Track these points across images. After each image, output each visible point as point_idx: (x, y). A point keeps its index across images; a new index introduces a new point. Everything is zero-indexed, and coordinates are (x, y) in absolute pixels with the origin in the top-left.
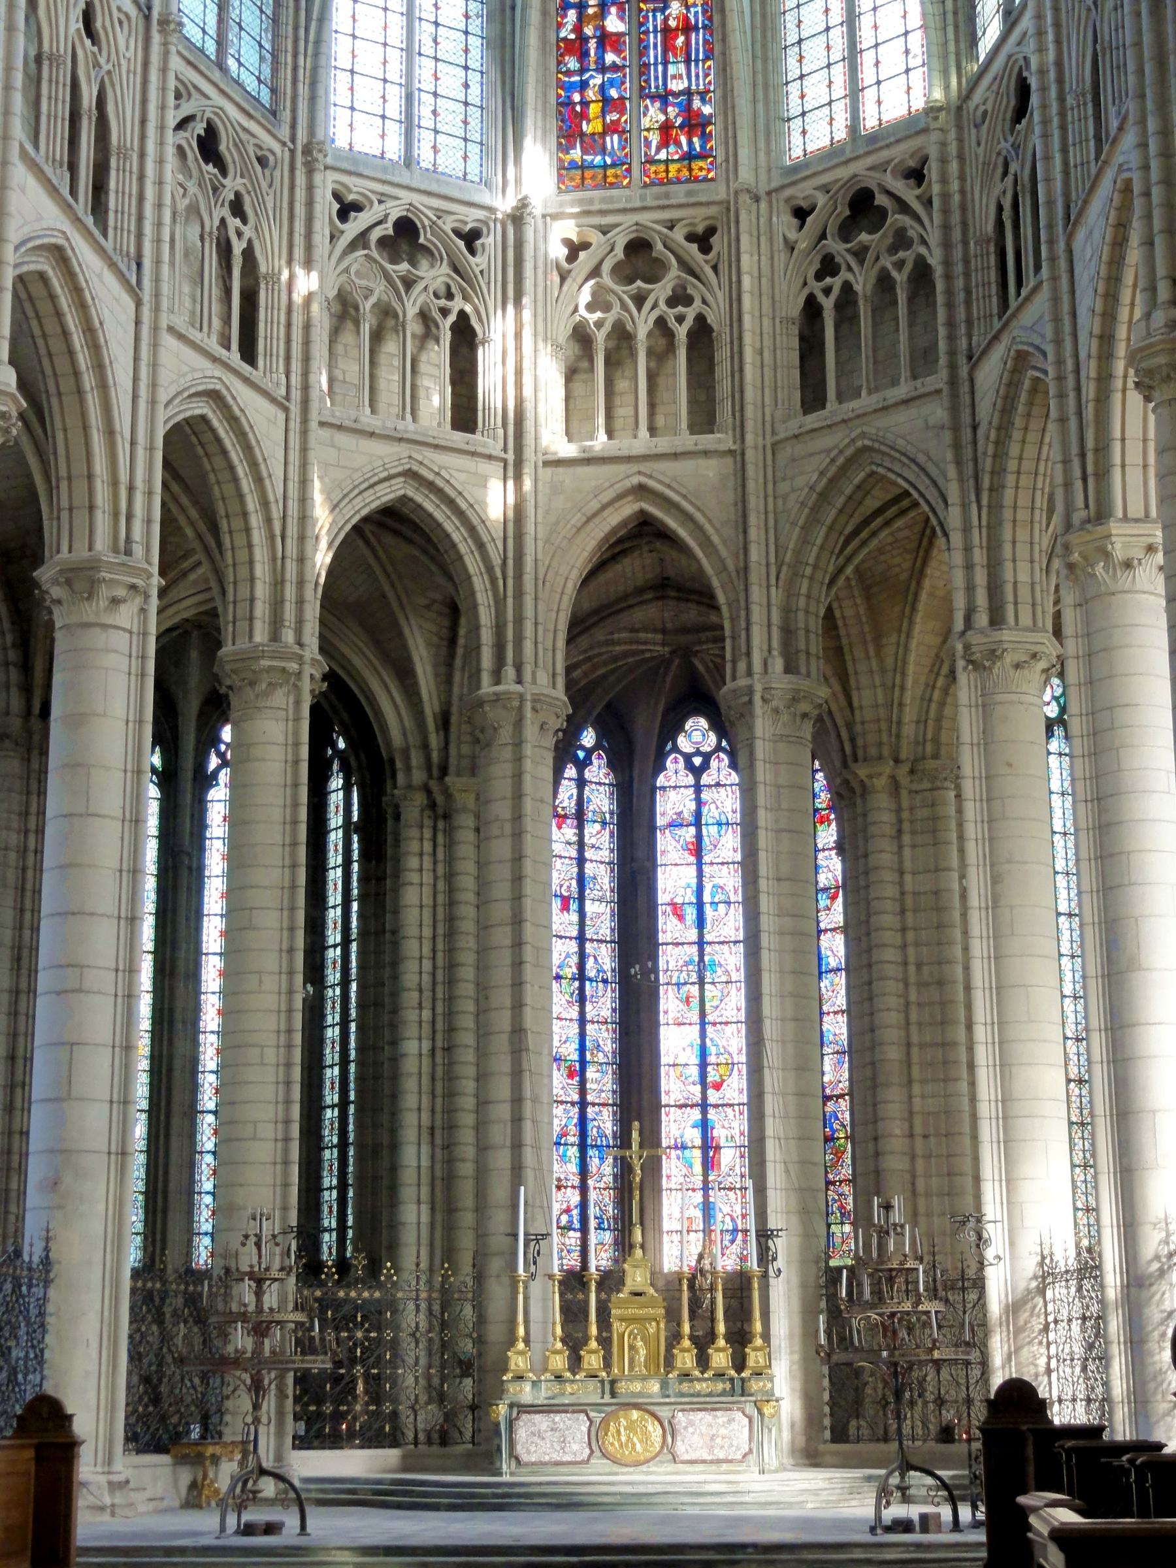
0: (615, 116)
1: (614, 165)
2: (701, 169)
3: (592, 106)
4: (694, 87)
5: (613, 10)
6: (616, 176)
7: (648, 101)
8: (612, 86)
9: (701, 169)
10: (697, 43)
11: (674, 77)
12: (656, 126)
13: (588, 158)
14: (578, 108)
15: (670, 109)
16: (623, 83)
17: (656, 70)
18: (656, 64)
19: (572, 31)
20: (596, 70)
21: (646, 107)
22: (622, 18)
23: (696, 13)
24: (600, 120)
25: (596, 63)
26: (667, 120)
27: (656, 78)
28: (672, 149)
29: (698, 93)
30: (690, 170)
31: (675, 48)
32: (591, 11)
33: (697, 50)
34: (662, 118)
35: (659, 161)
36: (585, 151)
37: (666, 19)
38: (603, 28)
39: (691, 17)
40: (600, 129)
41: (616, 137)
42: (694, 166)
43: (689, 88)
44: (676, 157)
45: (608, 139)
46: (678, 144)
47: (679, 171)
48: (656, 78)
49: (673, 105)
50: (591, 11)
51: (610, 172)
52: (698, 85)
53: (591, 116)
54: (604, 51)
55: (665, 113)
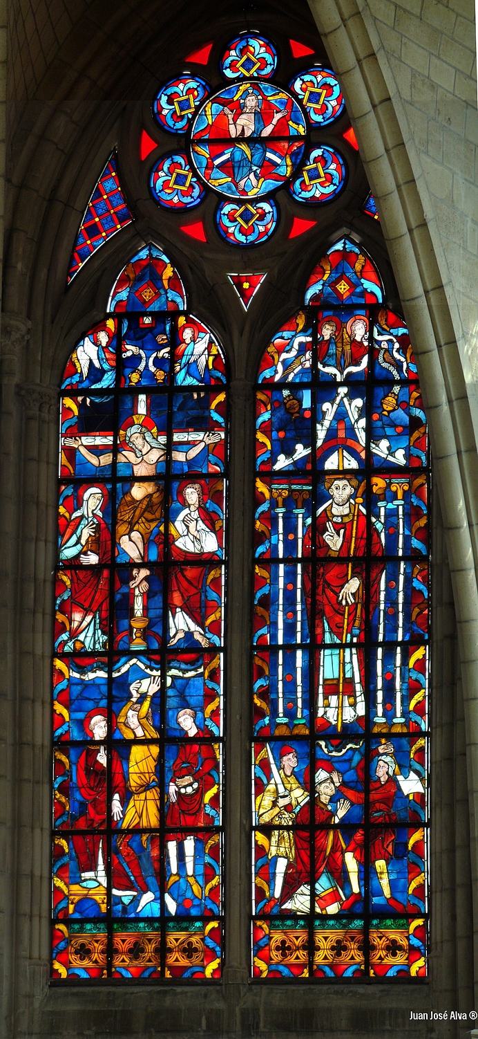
2: (393, 948)
6: (189, 951)
12: (287, 819)
13: (126, 896)
14: (102, 758)
23: (392, 514)
25: (146, 634)
26: (314, 801)
27: (290, 685)
32: (138, 492)
33: (391, 617)
37: (317, 529)
38: (167, 541)
43: (367, 719)
45: (172, 846)
46: (341, 876)
47: (339, 948)
48: (290, 685)
50: (138, 492)
51: (175, 938)
52: (390, 714)
53: (134, 781)
55: (310, 786)
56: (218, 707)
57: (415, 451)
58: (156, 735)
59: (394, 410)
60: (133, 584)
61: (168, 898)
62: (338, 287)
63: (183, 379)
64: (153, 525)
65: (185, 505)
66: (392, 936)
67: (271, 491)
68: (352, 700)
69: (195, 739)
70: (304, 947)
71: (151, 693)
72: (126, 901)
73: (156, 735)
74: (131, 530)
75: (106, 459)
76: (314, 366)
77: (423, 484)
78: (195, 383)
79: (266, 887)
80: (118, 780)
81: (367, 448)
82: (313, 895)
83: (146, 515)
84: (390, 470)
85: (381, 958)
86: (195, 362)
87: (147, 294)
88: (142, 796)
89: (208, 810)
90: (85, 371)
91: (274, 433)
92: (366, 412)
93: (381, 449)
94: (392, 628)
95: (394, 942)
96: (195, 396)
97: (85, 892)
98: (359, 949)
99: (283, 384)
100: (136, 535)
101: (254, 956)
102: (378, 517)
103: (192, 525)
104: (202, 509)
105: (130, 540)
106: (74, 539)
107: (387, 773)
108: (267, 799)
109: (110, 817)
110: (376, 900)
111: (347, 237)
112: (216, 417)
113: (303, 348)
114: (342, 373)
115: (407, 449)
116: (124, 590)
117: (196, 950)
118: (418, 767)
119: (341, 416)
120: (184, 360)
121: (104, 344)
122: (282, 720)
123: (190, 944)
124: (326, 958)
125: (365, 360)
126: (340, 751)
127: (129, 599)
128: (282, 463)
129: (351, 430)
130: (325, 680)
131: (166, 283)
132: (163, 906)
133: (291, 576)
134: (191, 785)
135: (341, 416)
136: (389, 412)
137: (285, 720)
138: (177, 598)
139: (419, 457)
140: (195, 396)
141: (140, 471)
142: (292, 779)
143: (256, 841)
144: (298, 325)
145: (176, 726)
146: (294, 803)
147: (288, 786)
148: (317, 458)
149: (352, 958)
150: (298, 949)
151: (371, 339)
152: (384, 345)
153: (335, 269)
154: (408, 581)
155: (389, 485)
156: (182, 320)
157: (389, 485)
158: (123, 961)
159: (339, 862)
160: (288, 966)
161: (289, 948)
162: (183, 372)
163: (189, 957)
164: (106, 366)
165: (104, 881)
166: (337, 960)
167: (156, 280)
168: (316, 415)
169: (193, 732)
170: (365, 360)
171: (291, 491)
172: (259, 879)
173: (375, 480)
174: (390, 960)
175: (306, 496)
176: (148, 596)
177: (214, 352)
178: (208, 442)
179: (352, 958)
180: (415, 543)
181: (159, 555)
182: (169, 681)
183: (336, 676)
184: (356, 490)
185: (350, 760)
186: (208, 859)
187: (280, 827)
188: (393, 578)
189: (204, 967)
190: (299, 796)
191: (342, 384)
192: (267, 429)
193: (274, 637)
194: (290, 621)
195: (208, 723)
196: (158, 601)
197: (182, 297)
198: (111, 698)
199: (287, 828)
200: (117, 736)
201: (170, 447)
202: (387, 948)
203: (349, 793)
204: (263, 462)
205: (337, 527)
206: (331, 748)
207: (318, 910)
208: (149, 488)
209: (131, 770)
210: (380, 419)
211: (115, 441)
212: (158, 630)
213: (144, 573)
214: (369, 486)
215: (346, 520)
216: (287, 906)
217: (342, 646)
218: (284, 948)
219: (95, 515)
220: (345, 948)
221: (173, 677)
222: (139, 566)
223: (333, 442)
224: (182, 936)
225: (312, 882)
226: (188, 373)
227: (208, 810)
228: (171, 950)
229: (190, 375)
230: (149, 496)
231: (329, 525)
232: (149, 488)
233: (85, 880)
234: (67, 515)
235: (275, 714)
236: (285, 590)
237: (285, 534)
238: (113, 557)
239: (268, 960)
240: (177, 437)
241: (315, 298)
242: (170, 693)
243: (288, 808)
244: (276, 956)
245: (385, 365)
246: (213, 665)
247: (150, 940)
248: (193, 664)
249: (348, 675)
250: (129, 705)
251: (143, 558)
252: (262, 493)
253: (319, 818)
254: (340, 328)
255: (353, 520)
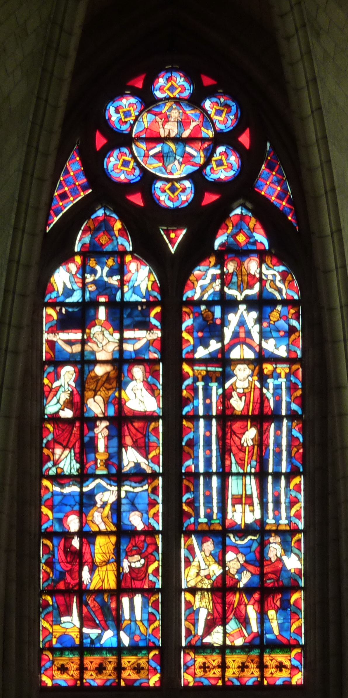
0: (137, 562)
1: (134, 649)
2: (280, 667)
3: (100, 541)
4: (270, 520)
5: (138, 371)
6: (138, 669)
7: (194, 540)
8: (134, 507)
9: (280, 667)
10: (278, 444)
11: (237, 500)
12: (207, 584)
13: (92, 633)
14: (76, 543)
15: (230, 556)
16: (153, 504)
17: (208, 486)
18: (208, 475)
19: (69, 404)
20: (108, 477)
21: (191, 549)
22: (151, 389)
23: (278, 387)
24: (112, 567)
25: (107, 464)
26: (225, 574)
27: (208, 499)
28: (232, 626)
29: (278, 532)
30: (262, 667)
31: (241, 448)
32: (100, 370)
33: (278, 455)
34: (216, 570)
35: (209, 648)
36: (85, 620)
37: (226, 397)
38: (120, 403)
39: (269, 394)
40: (111, 583)
41: (138, 599)
42: (267, 659)
43: (262, 522)
44: (239, 642)
45: (125, 601)
46: (244, 621)
47: (243, 667)
48: (208, 499)
49: (236, 549)
50: (100, 370)
51: (128, 660)
52: (277, 518)
53: (98, 558)
54: (121, 445)
55: (222, 563)
56: (158, 511)
57: (293, 348)
58: (113, 528)
59: (278, 320)
60: (96, 431)
61: (122, 634)
62: (238, 238)
63: (130, 297)
64: (111, 392)
65: (132, 378)
66: (280, 660)
67: (193, 370)
68: (251, 508)
69: (143, 532)
70: (219, 667)
71: (110, 502)
72: (93, 637)
73: (113, 528)
74: (95, 395)
75: (77, 348)
76: (222, 289)
77: (298, 369)
78: (139, 299)
79: (192, 628)
80: (87, 557)
81: (260, 345)
82: (225, 633)
83: (106, 385)
84: (276, 360)
85: (272, 673)
86: (139, 285)
87: (104, 239)
88: (104, 568)
89: (152, 578)
90: (61, 291)
91: (195, 334)
92: (259, 321)
93: (269, 346)
94: (278, 462)
95: (281, 663)
96: (140, 308)
97: (64, 630)
98: (257, 667)
99: (200, 302)
100: (98, 398)
101: (185, 672)
102: (268, 389)
103: (138, 393)
104: (146, 382)
105: (95, 401)
106: (55, 400)
107: (276, 555)
108: (193, 571)
109: (81, 582)
110: (269, 636)
111: (244, 206)
112: (154, 322)
113: (214, 278)
114: (241, 294)
115: (288, 346)
116: (91, 434)
117: (143, 668)
118: (297, 551)
119: (242, 323)
120: (131, 284)
121: (74, 273)
122: (202, 519)
123: (139, 665)
124: (234, 673)
125: (257, 287)
126: (243, 540)
127: (93, 441)
128: (201, 353)
129: (248, 333)
130: (232, 495)
131: (116, 233)
132: (119, 641)
133: (208, 427)
134: (139, 561)
135: (242, 323)
136: (274, 322)
137: (206, 520)
138: (128, 440)
139: (295, 352)
140: (140, 308)
141: (100, 356)
142: (211, 559)
143: (185, 598)
144: (210, 262)
145: (129, 523)
146: (212, 574)
147: (208, 563)
148: (224, 351)
149: (252, 673)
150: (214, 668)
151: (261, 273)
152: (270, 277)
153: (235, 226)
154: (289, 431)
155: (275, 369)
156: (128, 258)
157: (275, 369)
158: (91, 675)
159: (243, 612)
160: (208, 679)
161: (208, 667)
162: (130, 291)
163: (138, 673)
164: (75, 287)
165: (78, 624)
166: (242, 675)
167: (109, 231)
168: (224, 322)
169: (140, 526)
170: (257, 287)
171: (207, 371)
172: (187, 623)
173: (265, 366)
174: (278, 674)
175: (218, 375)
176: (109, 438)
177: (152, 279)
178: (149, 338)
179: (252, 673)
180: (294, 407)
181: (115, 412)
182: (123, 495)
183: (240, 493)
184: (253, 371)
185: (250, 547)
186: (150, 610)
187: (202, 590)
188: (279, 428)
189: (149, 679)
190: (216, 570)
191: (242, 302)
192: (190, 331)
193: (197, 467)
194: (208, 456)
195: (152, 521)
196: (115, 442)
197: (129, 242)
198: (81, 504)
199: (207, 590)
200: (86, 529)
201: (122, 341)
202: (277, 667)
203: (251, 568)
204: (188, 353)
205: (240, 396)
206: (237, 538)
207: (228, 643)
208: (108, 368)
209: (96, 551)
210: (269, 326)
211: (83, 336)
212: (115, 461)
213: (105, 424)
214: (261, 370)
215: (246, 391)
216: (207, 640)
217: (244, 475)
218: (205, 667)
219: (69, 385)
220: (247, 667)
221: (127, 492)
222: (101, 419)
223: (237, 340)
224: (133, 659)
225: (224, 623)
226: (134, 292)
227: (152, 578)
228: (124, 669)
229: (135, 294)
230: (108, 373)
231: (234, 394)
232: (108, 368)
233: (64, 622)
234: (50, 385)
235: (197, 516)
236: (205, 436)
237: (204, 399)
238: (82, 412)
239: (194, 675)
240: (128, 334)
241: (222, 245)
242: (124, 501)
243: (208, 577)
244: (199, 672)
245: (270, 290)
246: (154, 484)
247: (110, 662)
248: (140, 482)
249: (249, 493)
250: (95, 509)
251: (104, 414)
252: (187, 373)
253: (229, 583)
254: (240, 265)
255: (251, 392)
